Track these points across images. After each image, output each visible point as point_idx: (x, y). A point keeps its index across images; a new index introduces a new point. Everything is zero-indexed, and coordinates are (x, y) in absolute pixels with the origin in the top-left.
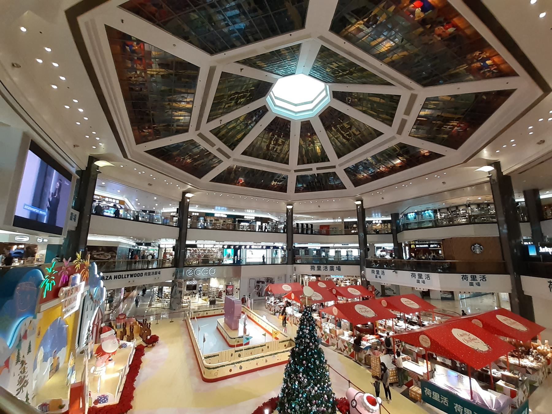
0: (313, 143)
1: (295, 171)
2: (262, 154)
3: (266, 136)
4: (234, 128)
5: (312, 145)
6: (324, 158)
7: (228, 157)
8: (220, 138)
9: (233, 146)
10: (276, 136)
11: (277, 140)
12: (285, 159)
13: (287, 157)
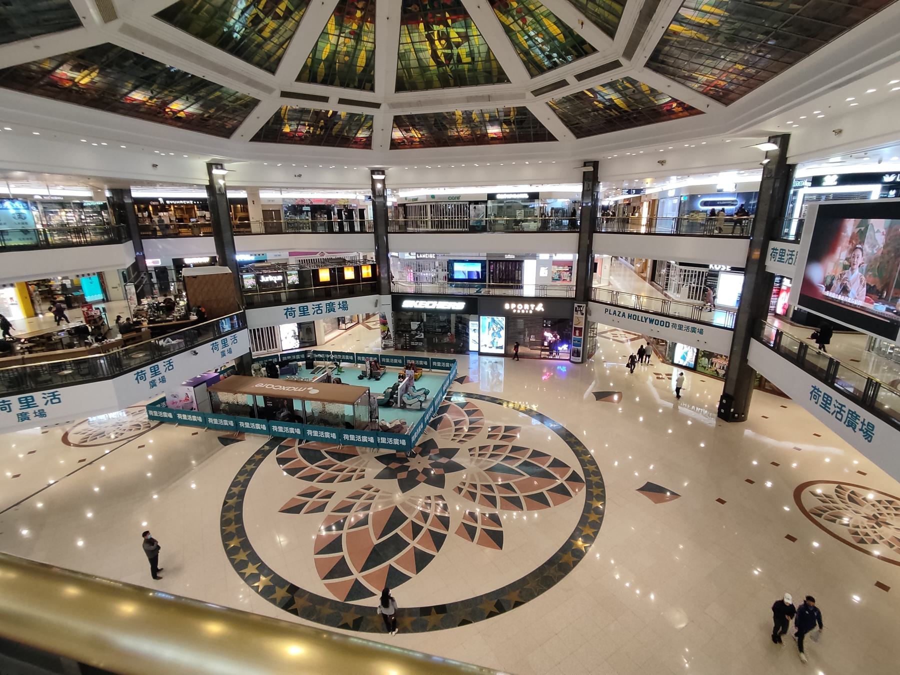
0: (530, 13)
1: (537, 93)
2: (435, 78)
3: (415, 36)
4: (334, 53)
5: (529, 19)
6: (581, 48)
7: (377, 106)
8: (328, 80)
9: (366, 81)
10: (435, 27)
11: (445, 36)
12: (495, 73)
13: (494, 64)
